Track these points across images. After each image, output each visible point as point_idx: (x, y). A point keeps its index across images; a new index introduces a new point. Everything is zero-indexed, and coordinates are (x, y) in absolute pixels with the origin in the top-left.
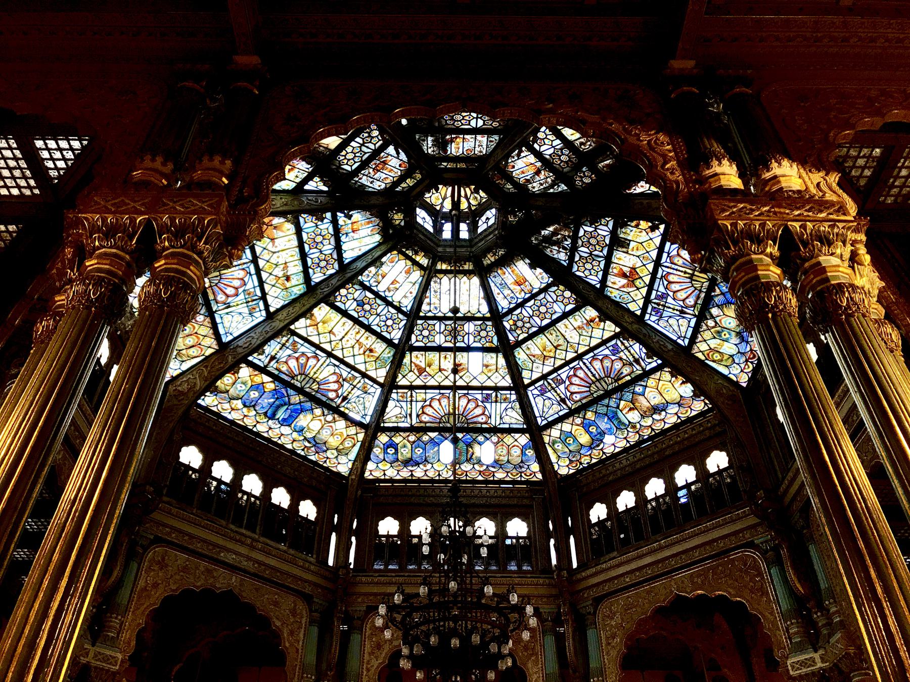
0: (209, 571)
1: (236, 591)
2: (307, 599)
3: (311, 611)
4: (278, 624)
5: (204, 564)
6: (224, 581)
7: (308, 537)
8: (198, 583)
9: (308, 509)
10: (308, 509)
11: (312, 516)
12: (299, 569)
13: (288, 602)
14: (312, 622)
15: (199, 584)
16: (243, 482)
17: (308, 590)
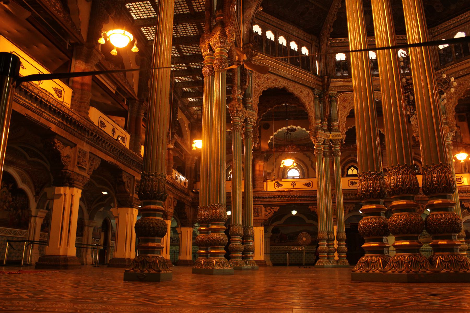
0: (276, 79)
1: (287, 87)
2: (312, 89)
3: (314, 94)
4: (304, 100)
5: (273, 77)
6: (281, 83)
7: (306, 64)
8: (273, 85)
9: (305, 51)
10: (305, 51)
11: (307, 54)
12: (306, 77)
13: (306, 91)
14: (315, 98)
15: (273, 85)
16: (279, 40)
17: (312, 86)
